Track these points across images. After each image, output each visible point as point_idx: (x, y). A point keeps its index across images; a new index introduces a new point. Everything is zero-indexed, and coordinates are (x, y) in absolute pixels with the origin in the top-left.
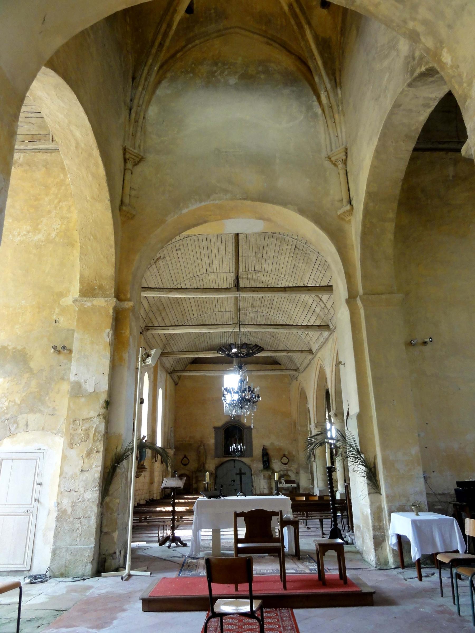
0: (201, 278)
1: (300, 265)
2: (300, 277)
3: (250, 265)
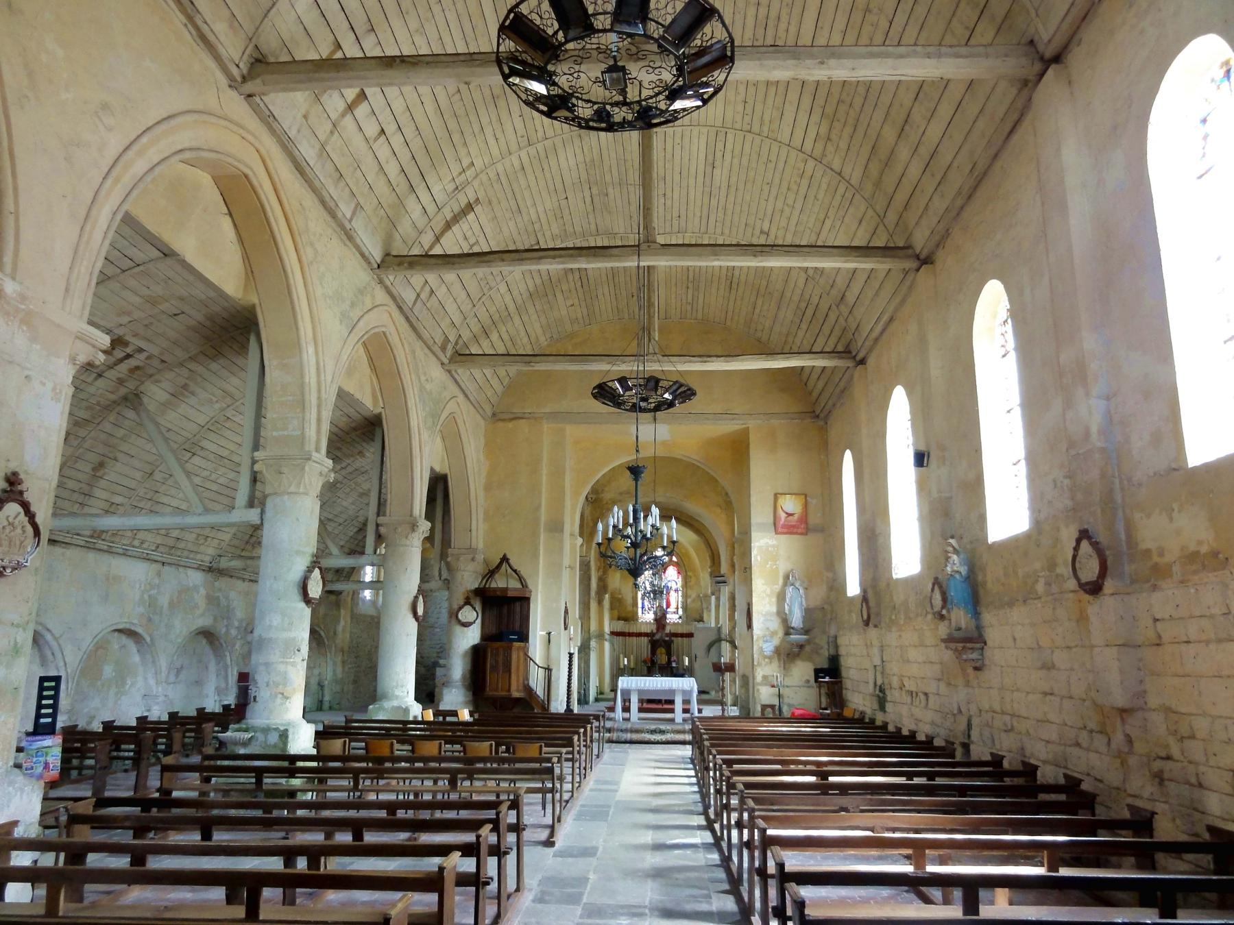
0: (747, 119)
1: (511, 224)
3: (613, 155)
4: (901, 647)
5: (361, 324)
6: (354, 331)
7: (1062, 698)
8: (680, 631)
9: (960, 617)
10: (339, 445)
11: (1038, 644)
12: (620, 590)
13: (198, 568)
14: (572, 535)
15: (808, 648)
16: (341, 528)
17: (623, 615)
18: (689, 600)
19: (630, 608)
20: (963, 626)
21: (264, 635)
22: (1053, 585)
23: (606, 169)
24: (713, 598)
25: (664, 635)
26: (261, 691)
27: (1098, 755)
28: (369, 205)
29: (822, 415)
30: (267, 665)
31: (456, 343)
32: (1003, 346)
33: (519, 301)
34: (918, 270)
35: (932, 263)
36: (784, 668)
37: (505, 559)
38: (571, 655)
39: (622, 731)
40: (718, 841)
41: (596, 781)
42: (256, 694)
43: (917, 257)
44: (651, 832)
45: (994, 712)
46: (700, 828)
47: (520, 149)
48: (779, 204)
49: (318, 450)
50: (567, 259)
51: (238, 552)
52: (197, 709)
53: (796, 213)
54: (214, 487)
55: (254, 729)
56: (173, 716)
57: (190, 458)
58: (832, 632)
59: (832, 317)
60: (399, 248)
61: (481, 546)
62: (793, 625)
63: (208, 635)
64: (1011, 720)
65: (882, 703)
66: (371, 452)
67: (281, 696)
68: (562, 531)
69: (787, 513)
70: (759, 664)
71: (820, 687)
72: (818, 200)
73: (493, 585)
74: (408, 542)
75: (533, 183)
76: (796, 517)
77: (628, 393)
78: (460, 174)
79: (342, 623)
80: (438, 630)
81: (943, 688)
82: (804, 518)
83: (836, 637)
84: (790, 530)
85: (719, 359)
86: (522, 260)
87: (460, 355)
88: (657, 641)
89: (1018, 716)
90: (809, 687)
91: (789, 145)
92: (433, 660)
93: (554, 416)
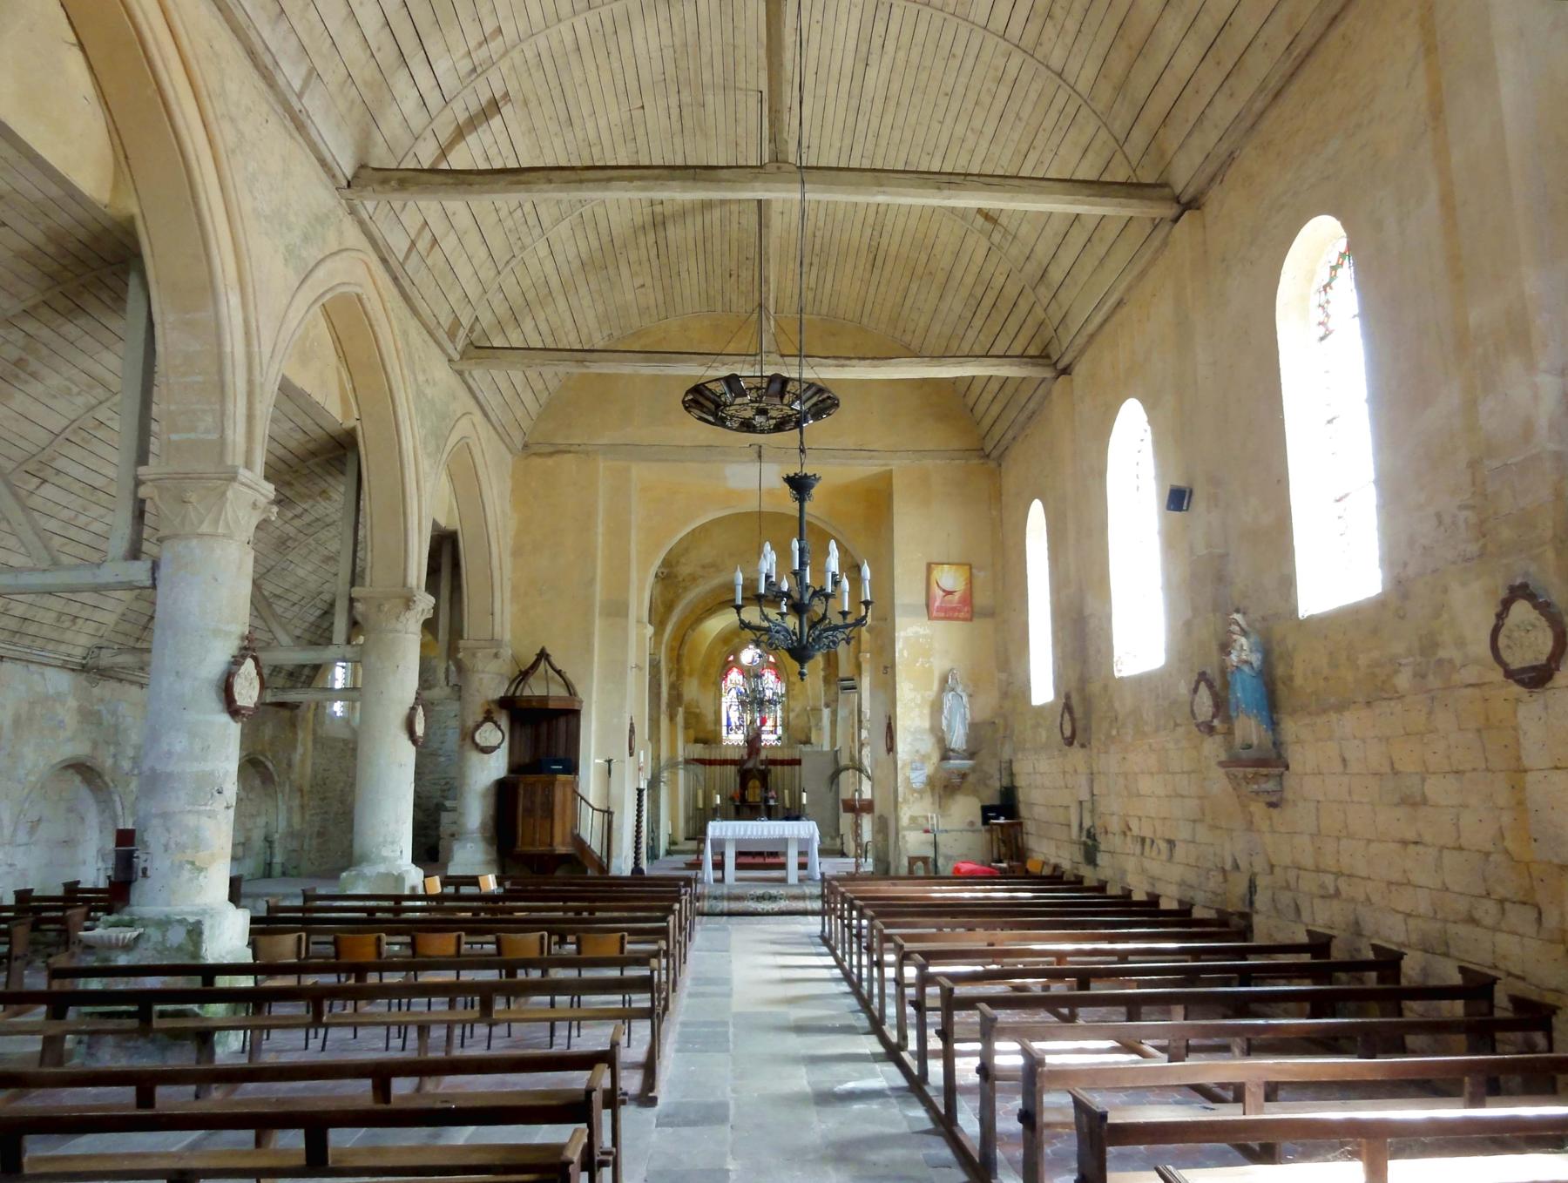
1: (558, 142)
2: (533, 104)
3: (716, 36)
4: (1126, 775)
5: (321, 273)
6: (309, 282)
7: (1442, 848)
8: (780, 756)
9: (1250, 728)
10: (287, 478)
11: (1393, 768)
12: (697, 702)
13: (64, 666)
14: (639, 621)
15: (971, 778)
16: (296, 608)
17: (701, 735)
18: (792, 715)
19: (710, 727)
20: (1255, 742)
21: (159, 767)
22: (1431, 677)
23: (705, 59)
24: (826, 712)
25: (758, 764)
26: (154, 858)
27: (1516, 939)
28: (333, 76)
29: (995, 454)
30: (165, 816)
31: (472, 330)
32: (1320, 324)
33: (565, 270)
34: (1176, 220)
35: (1198, 208)
36: (940, 807)
37: (543, 655)
38: (640, 791)
39: (715, 898)
40: (916, 1085)
41: (693, 979)
42: (147, 865)
43: (1177, 200)
44: (802, 1071)
45: (1299, 869)
46: (875, 1058)
47: (575, 13)
48: (960, 129)
49: (248, 465)
50: (652, 183)
51: (131, 643)
52: (65, 885)
53: (984, 144)
54: (84, 537)
55: (143, 922)
56: (23, 896)
57: (38, 487)
58: (1006, 756)
59: (1023, 306)
60: (381, 157)
61: (507, 637)
62: (953, 746)
63: (84, 770)
64: (1336, 880)
65: (1090, 853)
66: (340, 491)
67: (189, 866)
68: (627, 616)
69: (944, 591)
70: (906, 801)
71: (990, 831)
72: (1020, 119)
73: (527, 692)
74: (399, 626)
75: (592, 77)
76: (956, 597)
77: (738, 401)
78: (480, 45)
79: (300, 750)
80: (442, 759)
81: (1203, 834)
82: (968, 599)
83: (1011, 762)
84: (948, 614)
85: (863, 362)
86: (581, 181)
87: (477, 347)
88: (749, 771)
89: (1350, 876)
90: (973, 831)
91: (985, 28)
92: (435, 801)
93: (612, 449)
